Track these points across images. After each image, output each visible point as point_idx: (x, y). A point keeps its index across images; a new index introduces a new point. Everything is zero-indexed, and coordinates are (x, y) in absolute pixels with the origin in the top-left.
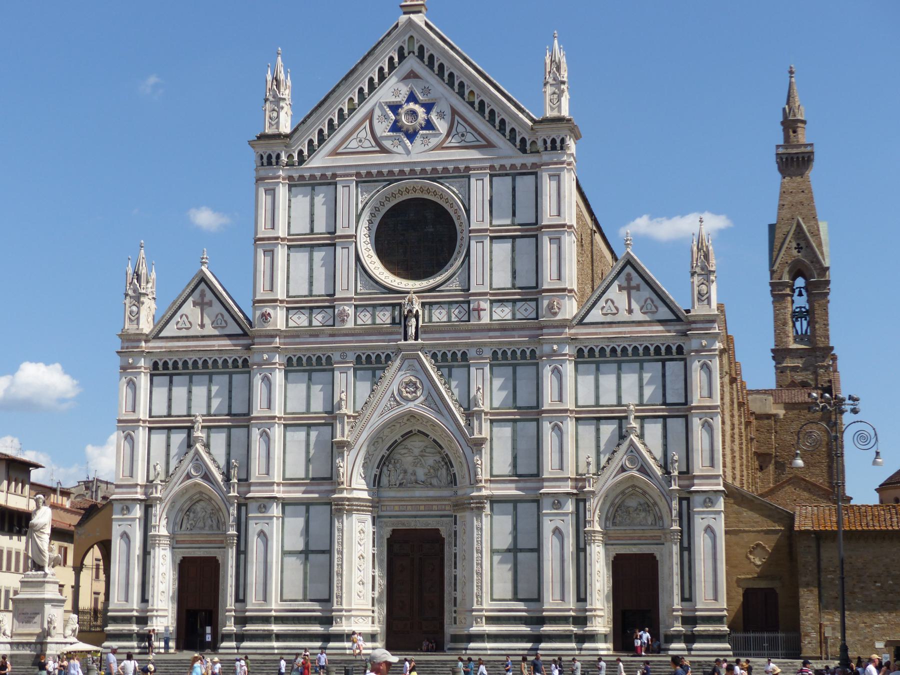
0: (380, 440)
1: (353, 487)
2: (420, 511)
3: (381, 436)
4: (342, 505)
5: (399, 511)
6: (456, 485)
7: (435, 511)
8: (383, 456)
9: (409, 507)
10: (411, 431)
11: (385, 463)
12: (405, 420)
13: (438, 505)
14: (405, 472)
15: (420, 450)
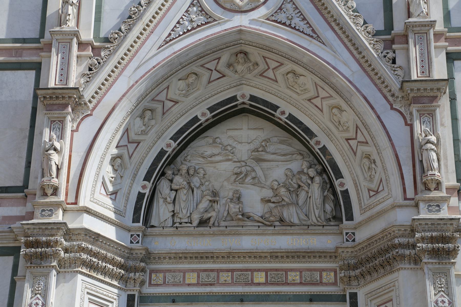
0: (159, 107)
1: (82, 203)
2: (252, 284)
3: (162, 97)
4: (48, 244)
5: (198, 284)
6: (350, 217)
7: (294, 284)
8: (162, 153)
9: (225, 277)
10: (234, 98)
11: (163, 174)
12: (222, 66)
13: (301, 271)
14: (215, 194)
15: (252, 147)
